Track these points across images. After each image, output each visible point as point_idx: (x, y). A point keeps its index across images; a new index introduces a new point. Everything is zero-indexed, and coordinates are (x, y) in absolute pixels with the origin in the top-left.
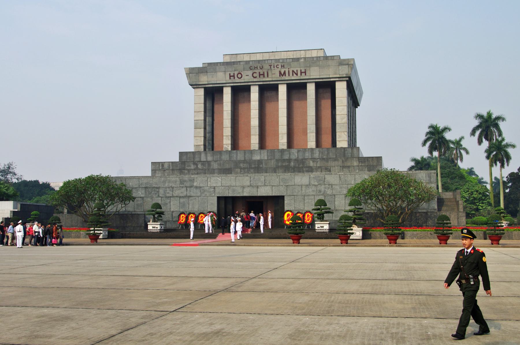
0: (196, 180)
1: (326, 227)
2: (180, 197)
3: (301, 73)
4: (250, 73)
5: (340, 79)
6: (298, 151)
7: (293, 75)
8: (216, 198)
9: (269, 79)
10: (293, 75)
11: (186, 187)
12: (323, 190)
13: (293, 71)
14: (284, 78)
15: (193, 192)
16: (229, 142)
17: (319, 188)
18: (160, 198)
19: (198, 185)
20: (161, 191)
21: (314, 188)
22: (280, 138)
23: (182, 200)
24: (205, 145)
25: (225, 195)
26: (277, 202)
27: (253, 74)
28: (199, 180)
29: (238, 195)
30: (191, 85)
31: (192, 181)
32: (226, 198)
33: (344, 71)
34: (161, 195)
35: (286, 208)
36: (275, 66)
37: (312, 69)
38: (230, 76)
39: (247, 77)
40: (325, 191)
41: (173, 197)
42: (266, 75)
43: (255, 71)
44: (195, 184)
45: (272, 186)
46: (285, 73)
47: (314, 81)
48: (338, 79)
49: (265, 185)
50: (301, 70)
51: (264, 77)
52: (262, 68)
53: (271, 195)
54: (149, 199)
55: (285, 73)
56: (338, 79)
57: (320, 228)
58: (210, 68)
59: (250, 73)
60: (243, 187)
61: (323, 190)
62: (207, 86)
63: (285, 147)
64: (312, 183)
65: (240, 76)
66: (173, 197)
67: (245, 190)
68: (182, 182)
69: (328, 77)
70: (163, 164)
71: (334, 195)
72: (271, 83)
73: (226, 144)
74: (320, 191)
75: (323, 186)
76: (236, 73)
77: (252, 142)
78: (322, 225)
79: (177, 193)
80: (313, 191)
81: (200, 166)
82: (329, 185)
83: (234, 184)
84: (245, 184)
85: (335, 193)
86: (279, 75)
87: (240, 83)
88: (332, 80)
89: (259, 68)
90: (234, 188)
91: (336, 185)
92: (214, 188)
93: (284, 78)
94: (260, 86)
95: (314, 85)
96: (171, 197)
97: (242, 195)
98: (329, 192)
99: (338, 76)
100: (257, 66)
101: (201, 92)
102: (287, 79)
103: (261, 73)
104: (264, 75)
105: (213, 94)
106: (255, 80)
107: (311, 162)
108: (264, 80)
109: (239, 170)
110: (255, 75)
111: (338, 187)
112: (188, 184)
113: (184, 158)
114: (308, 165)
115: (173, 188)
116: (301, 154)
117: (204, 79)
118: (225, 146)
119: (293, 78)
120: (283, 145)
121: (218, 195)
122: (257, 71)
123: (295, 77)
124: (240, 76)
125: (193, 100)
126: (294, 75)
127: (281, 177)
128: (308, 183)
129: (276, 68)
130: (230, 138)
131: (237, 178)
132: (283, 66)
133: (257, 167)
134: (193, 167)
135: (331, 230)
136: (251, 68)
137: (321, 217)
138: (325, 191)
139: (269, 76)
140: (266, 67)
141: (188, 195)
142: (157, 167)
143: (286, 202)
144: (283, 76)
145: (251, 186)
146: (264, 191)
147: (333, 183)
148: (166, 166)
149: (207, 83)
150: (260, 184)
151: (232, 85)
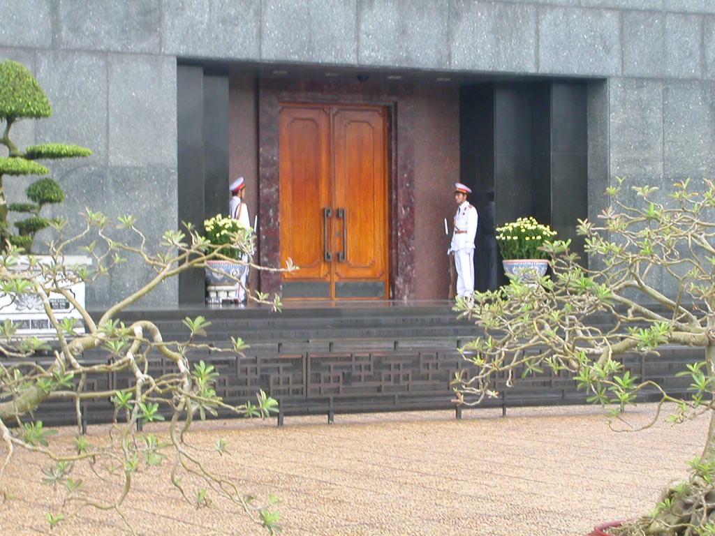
8: (170, 71)
29: (327, 56)
53: (531, 69)
97: (350, 59)
121: (183, 51)
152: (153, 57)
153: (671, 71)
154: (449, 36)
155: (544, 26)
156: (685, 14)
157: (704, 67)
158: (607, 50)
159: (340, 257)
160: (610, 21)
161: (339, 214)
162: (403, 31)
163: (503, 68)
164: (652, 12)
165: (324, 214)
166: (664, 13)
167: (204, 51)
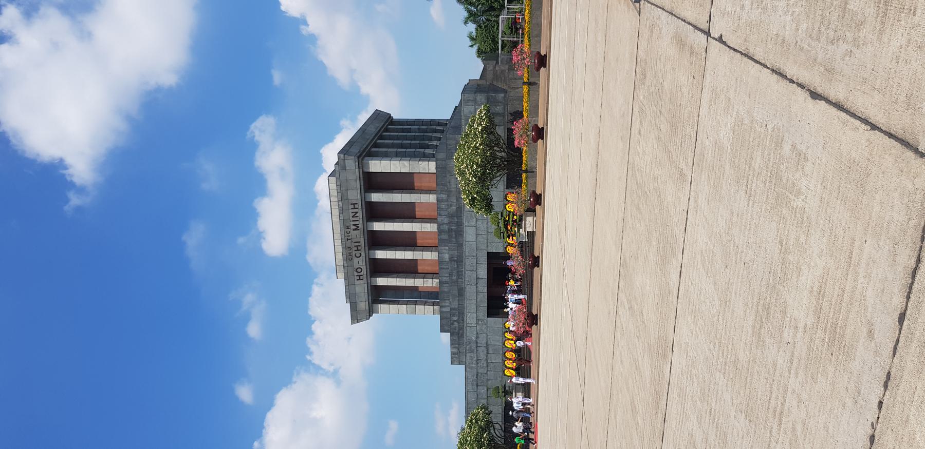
4: (356, 260)
6: (440, 215)
14: (361, 226)
15: (482, 340)
20: (480, 371)
21: (480, 222)
23: (491, 352)
24: (434, 304)
28: (470, 334)
30: (370, 316)
31: (470, 342)
33: (351, 163)
35: (501, 250)
37: (350, 198)
39: (361, 263)
41: (487, 360)
52: (351, 249)
54: (489, 383)
58: (351, 297)
59: (356, 260)
60: (477, 292)
63: (435, 226)
64: (473, 223)
65: (359, 270)
66: (487, 360)
68: (471, 351)
70: (452, 353)
76: (356, 274)
79: (482, 356)
81: (455, 318)
93: (361, 226)
100: (349, 252)
105: (378, 296)
109: (460, 280)
112: (474, 346)
113: (446, 328)
115: (477, 360)
116: (443, 213)
117: (363, 305)
122: (354, 253)
123: (360, 215)
125: (387, 312)
132: (348, 227)
134: (456, 325)
140: (349, 244)
142: (457, 357)
146: (483, 273)
148: (455, 351)
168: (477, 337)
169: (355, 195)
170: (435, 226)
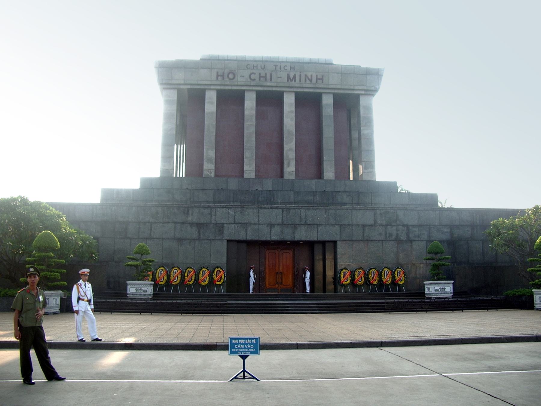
0: (190, 212)
1: (449, 289)
2: (163, 239)
3: (317, 79)
5: (366, 93)
7: (306, 81)
8: (225, 243)
9: (270, 85)
10: (306, 81)
11: (175, 223)
12: (394, 233)
13: (306, 76)
14: (293, 84)
16: (212, 167)
17: (390, 229)
18: (128, 241)
19: (195, 220)
22: (285, 166)
25: (241, 238)
26: (314, 250)
27: (250, 75)
32: (239, 242)
34: (130, 236)
36: (282, 67)
38: (218, 76)
39: (241, 80)
40: (397, 234)
41: (151, 238)
42: (268, 77)
43: (254, 71)
44: (190, 219)
45: (317, 225)
46: (295, 77)
47: (333, 91)
48: (363, 92)
49: (306, 224)
50: (317, 76)
51: (266, 79)
53: (316, 239)
55: (295, 77)
56: (363, 92)
57: (439, 291)
59: (246, 73)
60: (272, 225)
61: (394, 233)
62: (182, 87)
63: (293, 177)
64: (379, 222)
67: (273, 231)
69: (352, 88)
71: (411, 241)
72: (274, 89)
73: (208, 170)
74: (391, 235)
75: (395, 228)
76: (226, 71)
77: (246, 168)
78: (442, 286)
80: (381, 234)
82: (404, 226)
83: (254, 220)
84: (274, 222)
85: (413, 239)
86: (286, 79)
87: (231, 85)
88: (356, 92)
89: (259, 68)
90: (257, 226)
91: (413, 226)
92: (223, 227)
94: (258, 93)
95: (331, 97)
96: (147, 238)
97: (269, 239)
98: (403, 237)
99: (365, 88)
101: (174, 95)
102: (297, 85)
103: (263, 74)
104: (265, 77)
106: (253, 83)
107: (345, 196)
108: (265, 84)
110: (253, 77)
111: (416, 229)
114: (340, 200)
118: (205, 172)
119: (305, 85)
120: (289, 173)
121: (228, 238)
124: (231, 76)
126: (308, 81)
127: (331, 211)
128: (372, 222)
129: (283, 69)
130: (214, 161)
131: (262, 211)
133: (267, 201)
135: (456, 293)
136: (248, 67)
137: (438, 274)
138: (397, 234)
139: (273, 80)
141: (178, 235)
143: (339, 251)
144: (292, 81)
145: (282, 224)
147: (410, 223)
149: (182, 82)
150: (297, 221)
151: (219, 87)
152: (221, 240)
153: (354, 239)
154: (294, 233)
155: (319, 230)
156: (358, 225)
157: (363, 237)
158: (337, 235)
159: (281, 283)
160: (337, 228)
161: (281, 273)
162: (282, 232)
163: (308, 240)
164: (349, 225)
165: (277, 273)
166: (352, 225)
167: (233, 239)
168: (192, 224)
169: (334, 81)
170: (293, 177)
